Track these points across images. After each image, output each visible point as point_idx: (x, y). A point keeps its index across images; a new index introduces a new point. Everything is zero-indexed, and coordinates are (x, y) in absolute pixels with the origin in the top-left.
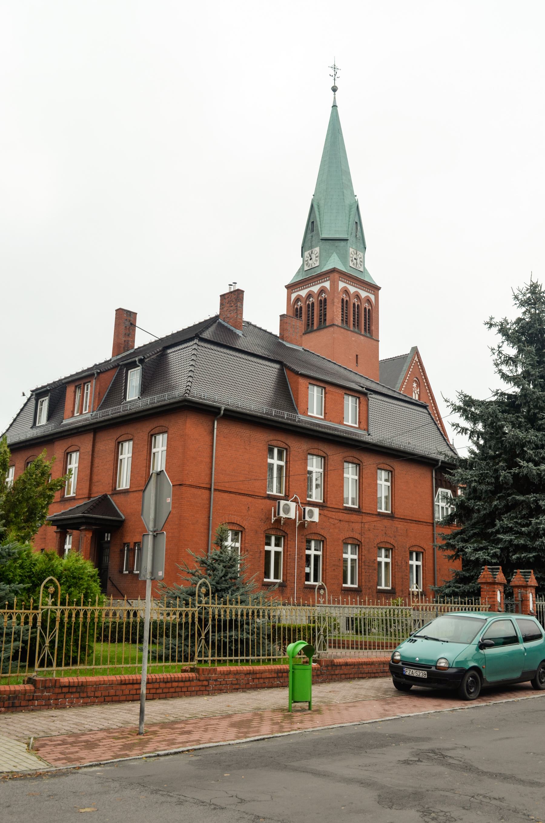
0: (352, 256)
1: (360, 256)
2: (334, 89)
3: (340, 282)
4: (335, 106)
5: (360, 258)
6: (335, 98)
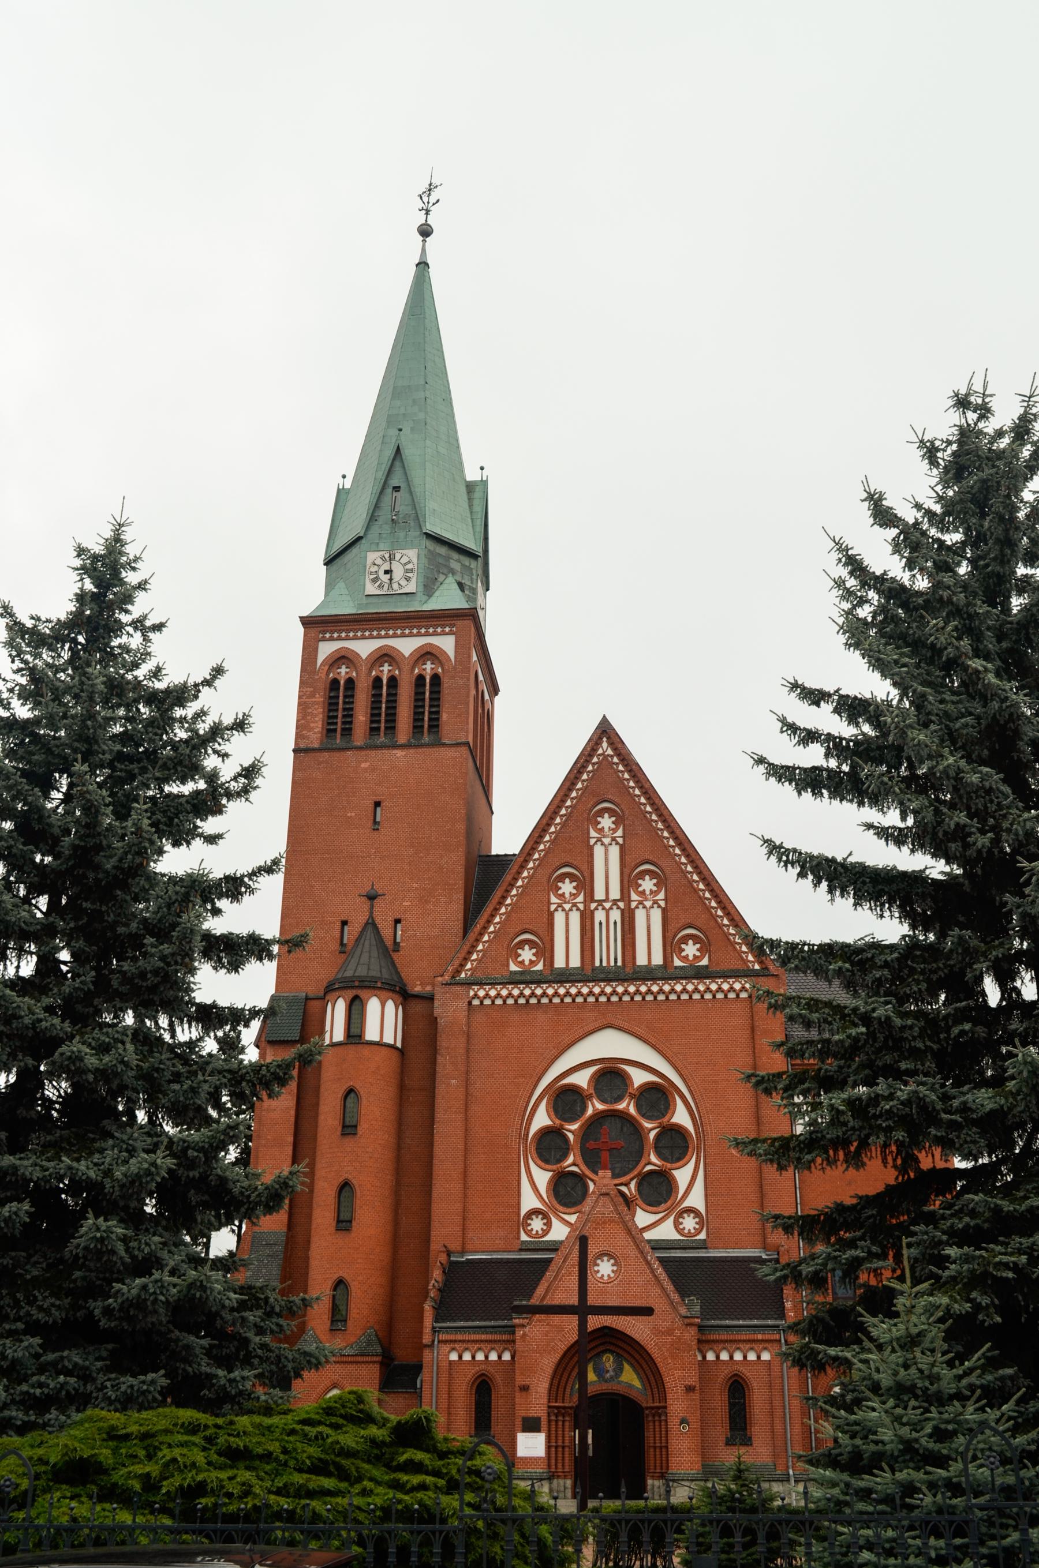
0: (374, 569)
1: (404, 560)
2: (425, 232)
3: (321, 645)
4: (423, 265)
5: (409, 562)
6: (424, 250)
